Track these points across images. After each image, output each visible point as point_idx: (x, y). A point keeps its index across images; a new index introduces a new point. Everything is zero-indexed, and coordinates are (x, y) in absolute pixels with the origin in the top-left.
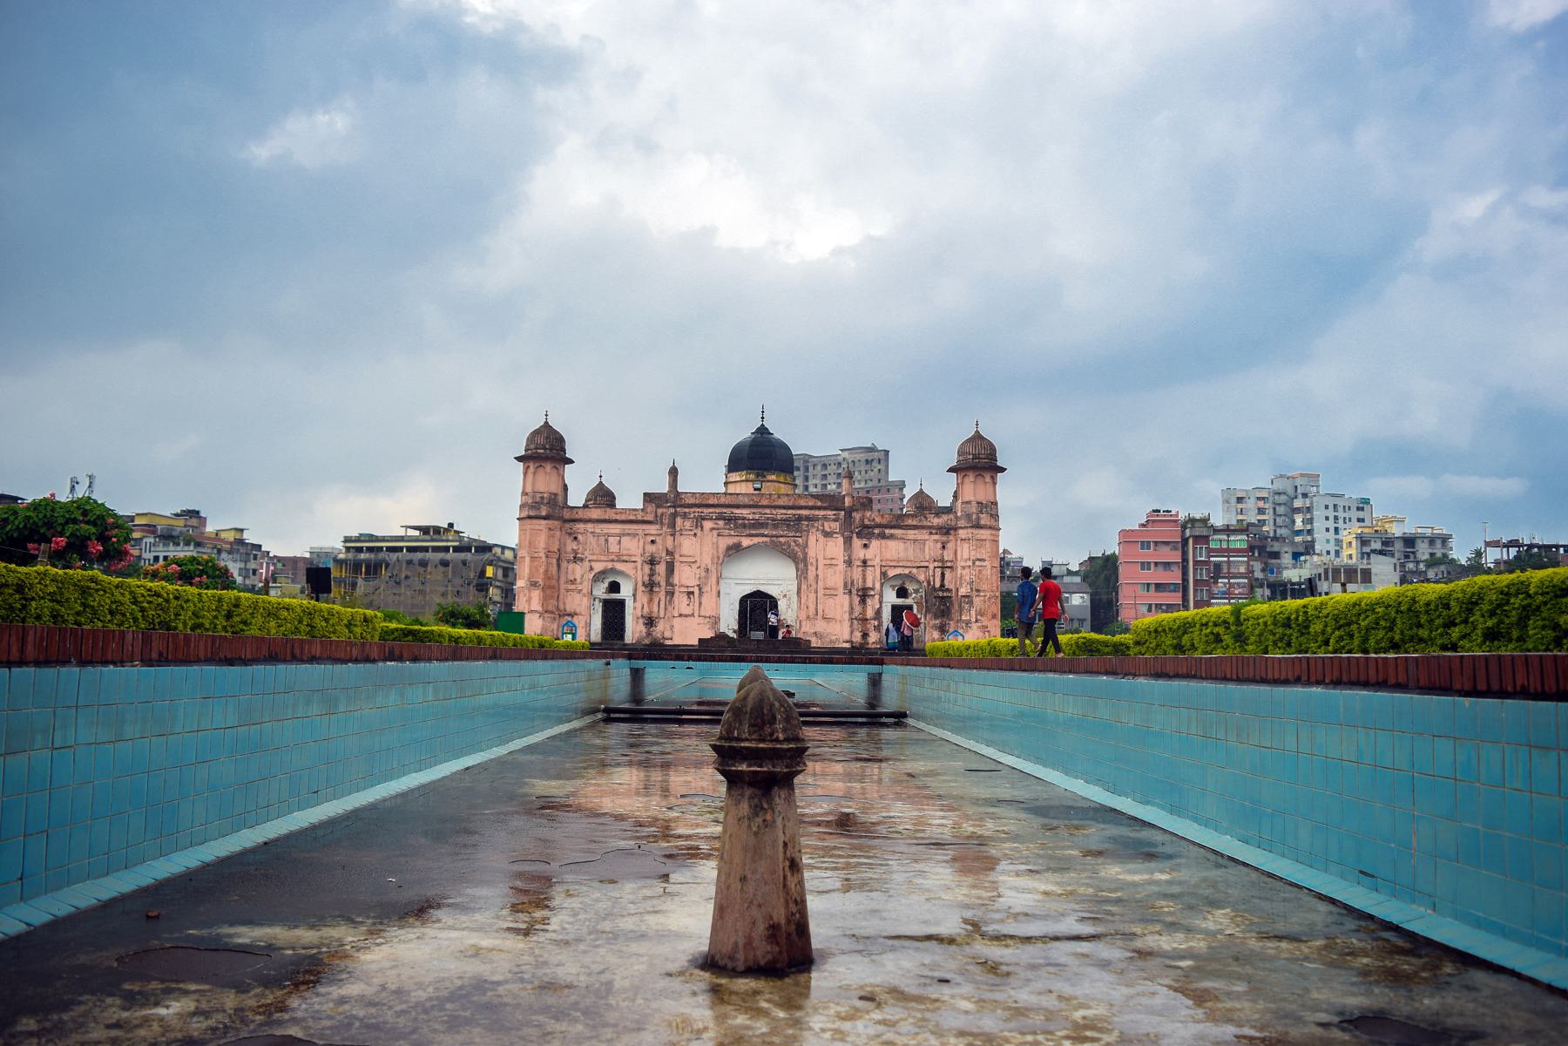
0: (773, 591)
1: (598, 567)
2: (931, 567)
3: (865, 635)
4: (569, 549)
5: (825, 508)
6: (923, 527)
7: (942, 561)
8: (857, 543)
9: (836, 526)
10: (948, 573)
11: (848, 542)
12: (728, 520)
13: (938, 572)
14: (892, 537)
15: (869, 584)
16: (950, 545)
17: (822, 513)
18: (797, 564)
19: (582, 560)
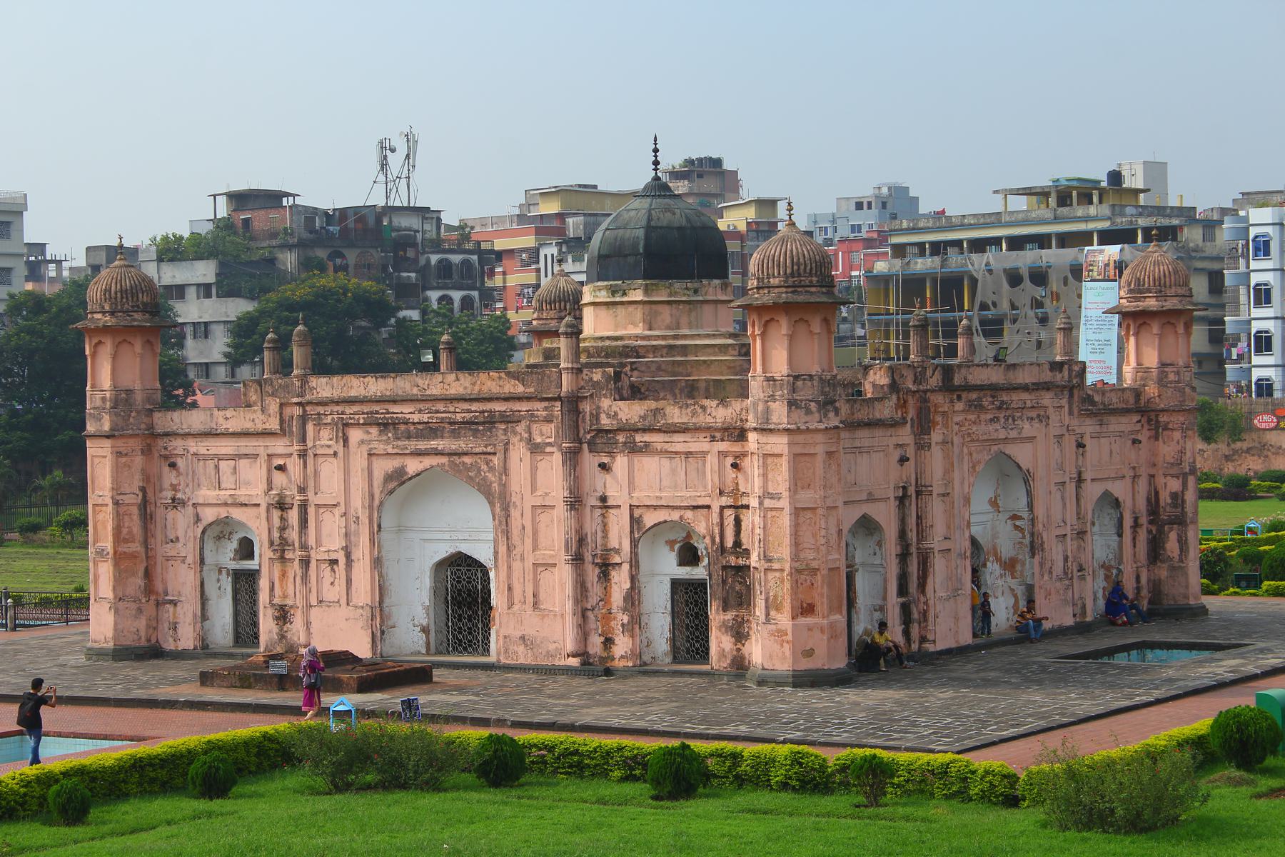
1: (209, 515)
3: (608, 642)
4: (166, 484)
5: (529, 399)
6: (697, 429)
7: (736, 493)
8: (590, 461)
9: (550, 429)
11: (572, 458)
12: (385, 426)
13: (730, 515)
14: (646, 449)
15: (614, 543)
17: (523, 407)
18: (492, 504)
19: (183, 503)
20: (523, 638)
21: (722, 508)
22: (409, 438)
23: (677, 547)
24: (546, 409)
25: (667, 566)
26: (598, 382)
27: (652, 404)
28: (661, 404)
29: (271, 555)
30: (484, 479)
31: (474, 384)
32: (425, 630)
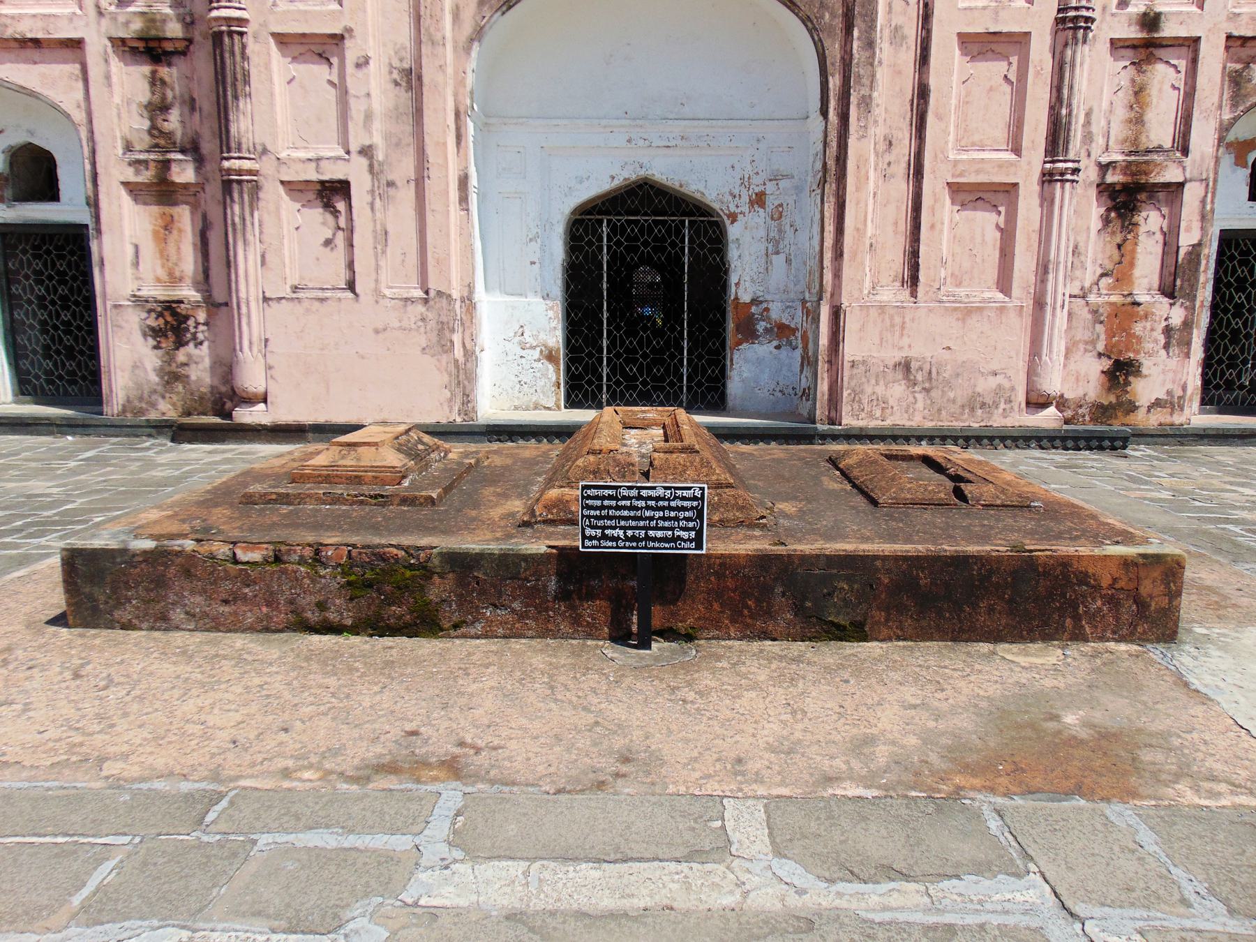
0: (703, 176)
3: (1121, 371)
20: (905, 367)
29: (130, 175)
32: (551, 357)
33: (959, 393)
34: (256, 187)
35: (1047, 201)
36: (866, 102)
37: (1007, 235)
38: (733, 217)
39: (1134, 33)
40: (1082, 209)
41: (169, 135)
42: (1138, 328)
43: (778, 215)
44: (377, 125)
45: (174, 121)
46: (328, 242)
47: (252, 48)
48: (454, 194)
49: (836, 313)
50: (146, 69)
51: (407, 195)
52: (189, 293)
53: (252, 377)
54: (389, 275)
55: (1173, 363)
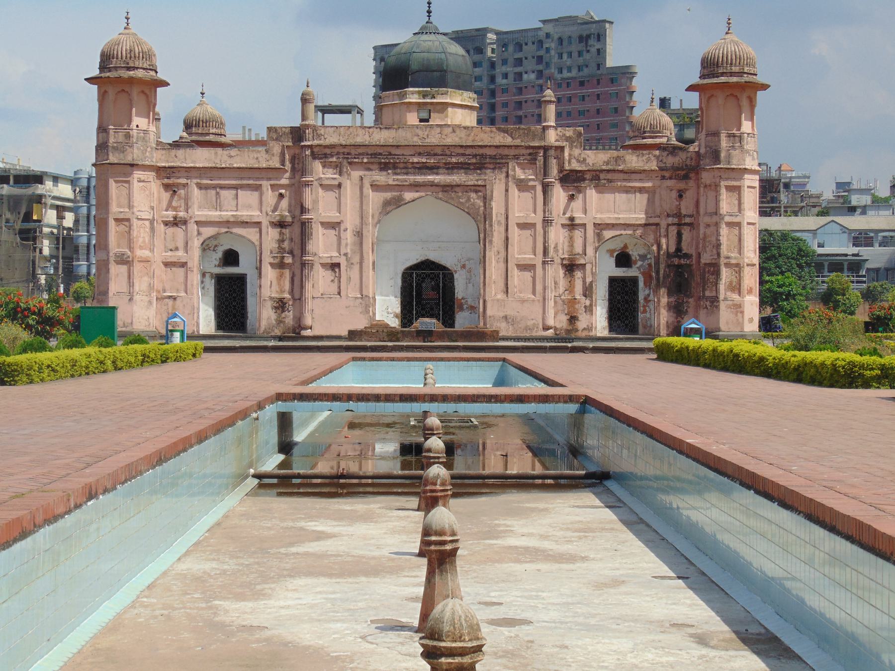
2: (663, 224)
3: (573, 319)
7: (678, 215)
10: (686, 234)
13: (673, 230)
16: (690, 195)
17: (512, 152)
20: (506, 317)
21: (669, 225)
22: (407, 174)
23: (615, 255)
24: (530, 154)
25: (605, 269)
26: (570, 137)
27: (615, 153)
28: (622, 152)
30: (473, 204)
31: (469, 135)
32: (397, 316)
33: (522, 325)
34: (313, 264)
35: (544, 269)
36: (491, 242)
37: (534, 278)
38: (456, 272)
39: (567, 222)
40: (556, 272)
41: (284, 249)
42: (577, 306)
43: (470, 271)
44: (349, 247)
45: (286, 245)
46: (332, 281)
47: (314, 225)
48: (371, 267)
49: (485, 301)
50: (279, 230)
51: (356, 268)
52: (287, 296)
53: (308, 321)
54: (351, 291)
55: (588, 317)
